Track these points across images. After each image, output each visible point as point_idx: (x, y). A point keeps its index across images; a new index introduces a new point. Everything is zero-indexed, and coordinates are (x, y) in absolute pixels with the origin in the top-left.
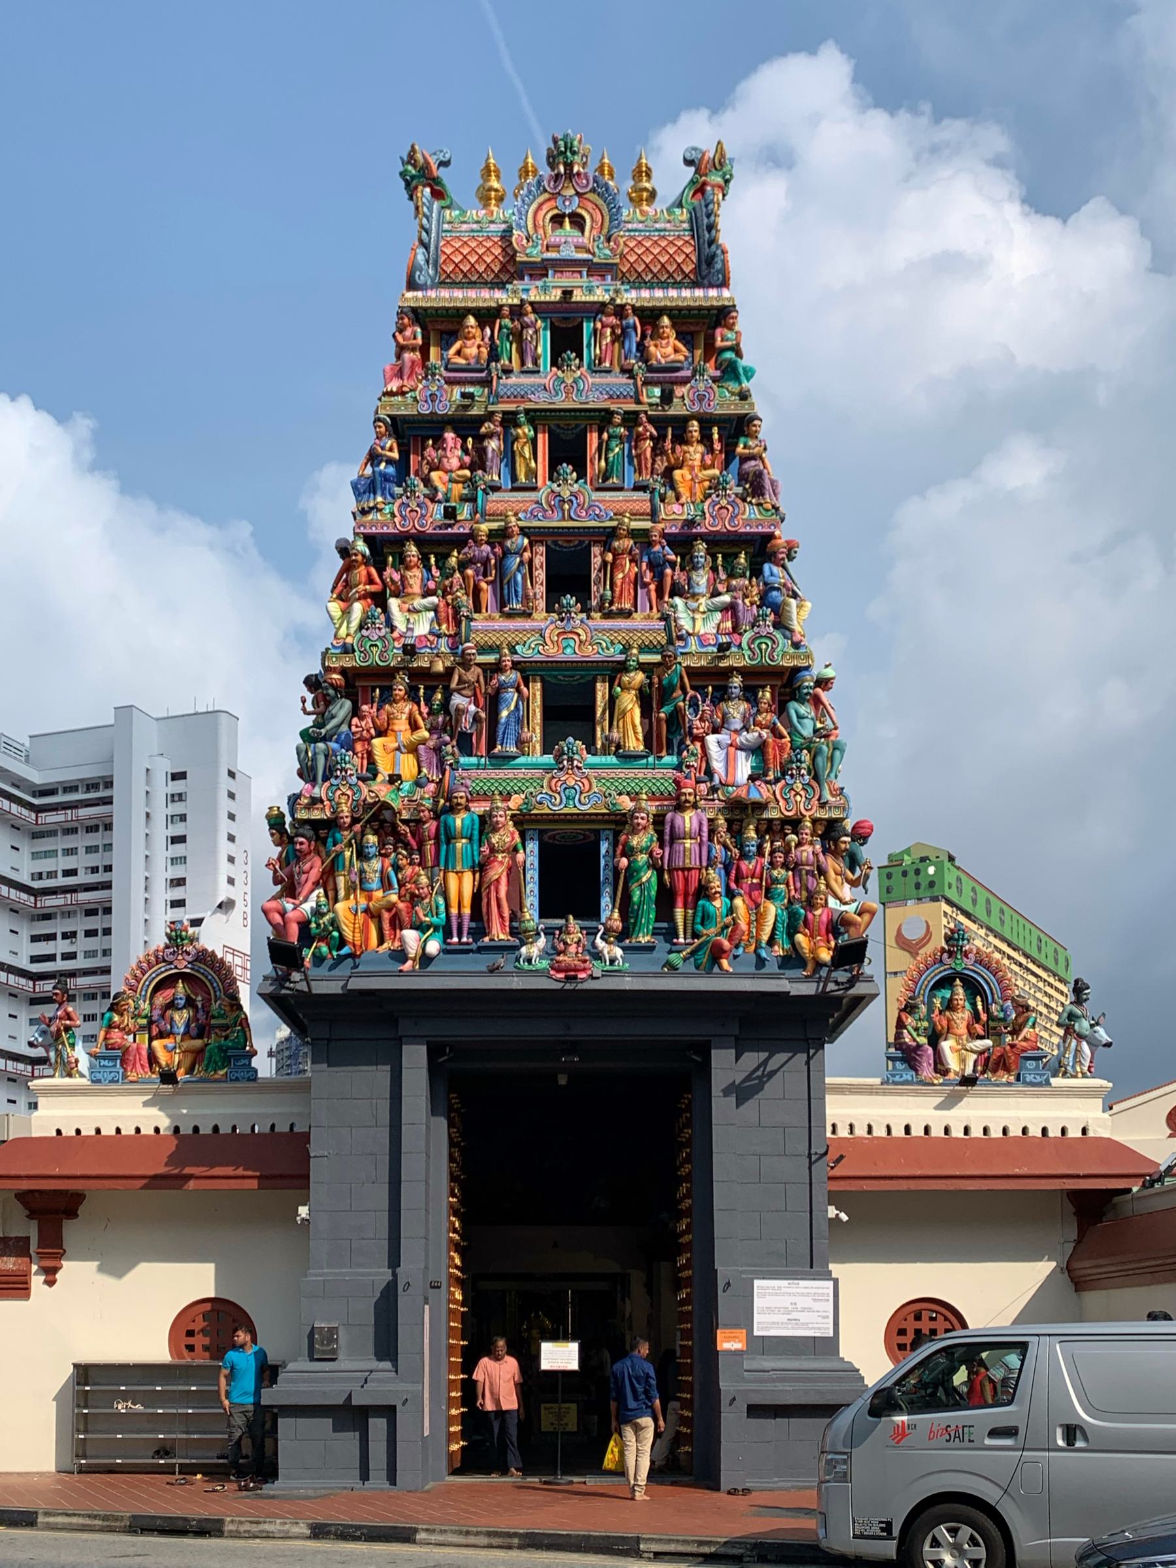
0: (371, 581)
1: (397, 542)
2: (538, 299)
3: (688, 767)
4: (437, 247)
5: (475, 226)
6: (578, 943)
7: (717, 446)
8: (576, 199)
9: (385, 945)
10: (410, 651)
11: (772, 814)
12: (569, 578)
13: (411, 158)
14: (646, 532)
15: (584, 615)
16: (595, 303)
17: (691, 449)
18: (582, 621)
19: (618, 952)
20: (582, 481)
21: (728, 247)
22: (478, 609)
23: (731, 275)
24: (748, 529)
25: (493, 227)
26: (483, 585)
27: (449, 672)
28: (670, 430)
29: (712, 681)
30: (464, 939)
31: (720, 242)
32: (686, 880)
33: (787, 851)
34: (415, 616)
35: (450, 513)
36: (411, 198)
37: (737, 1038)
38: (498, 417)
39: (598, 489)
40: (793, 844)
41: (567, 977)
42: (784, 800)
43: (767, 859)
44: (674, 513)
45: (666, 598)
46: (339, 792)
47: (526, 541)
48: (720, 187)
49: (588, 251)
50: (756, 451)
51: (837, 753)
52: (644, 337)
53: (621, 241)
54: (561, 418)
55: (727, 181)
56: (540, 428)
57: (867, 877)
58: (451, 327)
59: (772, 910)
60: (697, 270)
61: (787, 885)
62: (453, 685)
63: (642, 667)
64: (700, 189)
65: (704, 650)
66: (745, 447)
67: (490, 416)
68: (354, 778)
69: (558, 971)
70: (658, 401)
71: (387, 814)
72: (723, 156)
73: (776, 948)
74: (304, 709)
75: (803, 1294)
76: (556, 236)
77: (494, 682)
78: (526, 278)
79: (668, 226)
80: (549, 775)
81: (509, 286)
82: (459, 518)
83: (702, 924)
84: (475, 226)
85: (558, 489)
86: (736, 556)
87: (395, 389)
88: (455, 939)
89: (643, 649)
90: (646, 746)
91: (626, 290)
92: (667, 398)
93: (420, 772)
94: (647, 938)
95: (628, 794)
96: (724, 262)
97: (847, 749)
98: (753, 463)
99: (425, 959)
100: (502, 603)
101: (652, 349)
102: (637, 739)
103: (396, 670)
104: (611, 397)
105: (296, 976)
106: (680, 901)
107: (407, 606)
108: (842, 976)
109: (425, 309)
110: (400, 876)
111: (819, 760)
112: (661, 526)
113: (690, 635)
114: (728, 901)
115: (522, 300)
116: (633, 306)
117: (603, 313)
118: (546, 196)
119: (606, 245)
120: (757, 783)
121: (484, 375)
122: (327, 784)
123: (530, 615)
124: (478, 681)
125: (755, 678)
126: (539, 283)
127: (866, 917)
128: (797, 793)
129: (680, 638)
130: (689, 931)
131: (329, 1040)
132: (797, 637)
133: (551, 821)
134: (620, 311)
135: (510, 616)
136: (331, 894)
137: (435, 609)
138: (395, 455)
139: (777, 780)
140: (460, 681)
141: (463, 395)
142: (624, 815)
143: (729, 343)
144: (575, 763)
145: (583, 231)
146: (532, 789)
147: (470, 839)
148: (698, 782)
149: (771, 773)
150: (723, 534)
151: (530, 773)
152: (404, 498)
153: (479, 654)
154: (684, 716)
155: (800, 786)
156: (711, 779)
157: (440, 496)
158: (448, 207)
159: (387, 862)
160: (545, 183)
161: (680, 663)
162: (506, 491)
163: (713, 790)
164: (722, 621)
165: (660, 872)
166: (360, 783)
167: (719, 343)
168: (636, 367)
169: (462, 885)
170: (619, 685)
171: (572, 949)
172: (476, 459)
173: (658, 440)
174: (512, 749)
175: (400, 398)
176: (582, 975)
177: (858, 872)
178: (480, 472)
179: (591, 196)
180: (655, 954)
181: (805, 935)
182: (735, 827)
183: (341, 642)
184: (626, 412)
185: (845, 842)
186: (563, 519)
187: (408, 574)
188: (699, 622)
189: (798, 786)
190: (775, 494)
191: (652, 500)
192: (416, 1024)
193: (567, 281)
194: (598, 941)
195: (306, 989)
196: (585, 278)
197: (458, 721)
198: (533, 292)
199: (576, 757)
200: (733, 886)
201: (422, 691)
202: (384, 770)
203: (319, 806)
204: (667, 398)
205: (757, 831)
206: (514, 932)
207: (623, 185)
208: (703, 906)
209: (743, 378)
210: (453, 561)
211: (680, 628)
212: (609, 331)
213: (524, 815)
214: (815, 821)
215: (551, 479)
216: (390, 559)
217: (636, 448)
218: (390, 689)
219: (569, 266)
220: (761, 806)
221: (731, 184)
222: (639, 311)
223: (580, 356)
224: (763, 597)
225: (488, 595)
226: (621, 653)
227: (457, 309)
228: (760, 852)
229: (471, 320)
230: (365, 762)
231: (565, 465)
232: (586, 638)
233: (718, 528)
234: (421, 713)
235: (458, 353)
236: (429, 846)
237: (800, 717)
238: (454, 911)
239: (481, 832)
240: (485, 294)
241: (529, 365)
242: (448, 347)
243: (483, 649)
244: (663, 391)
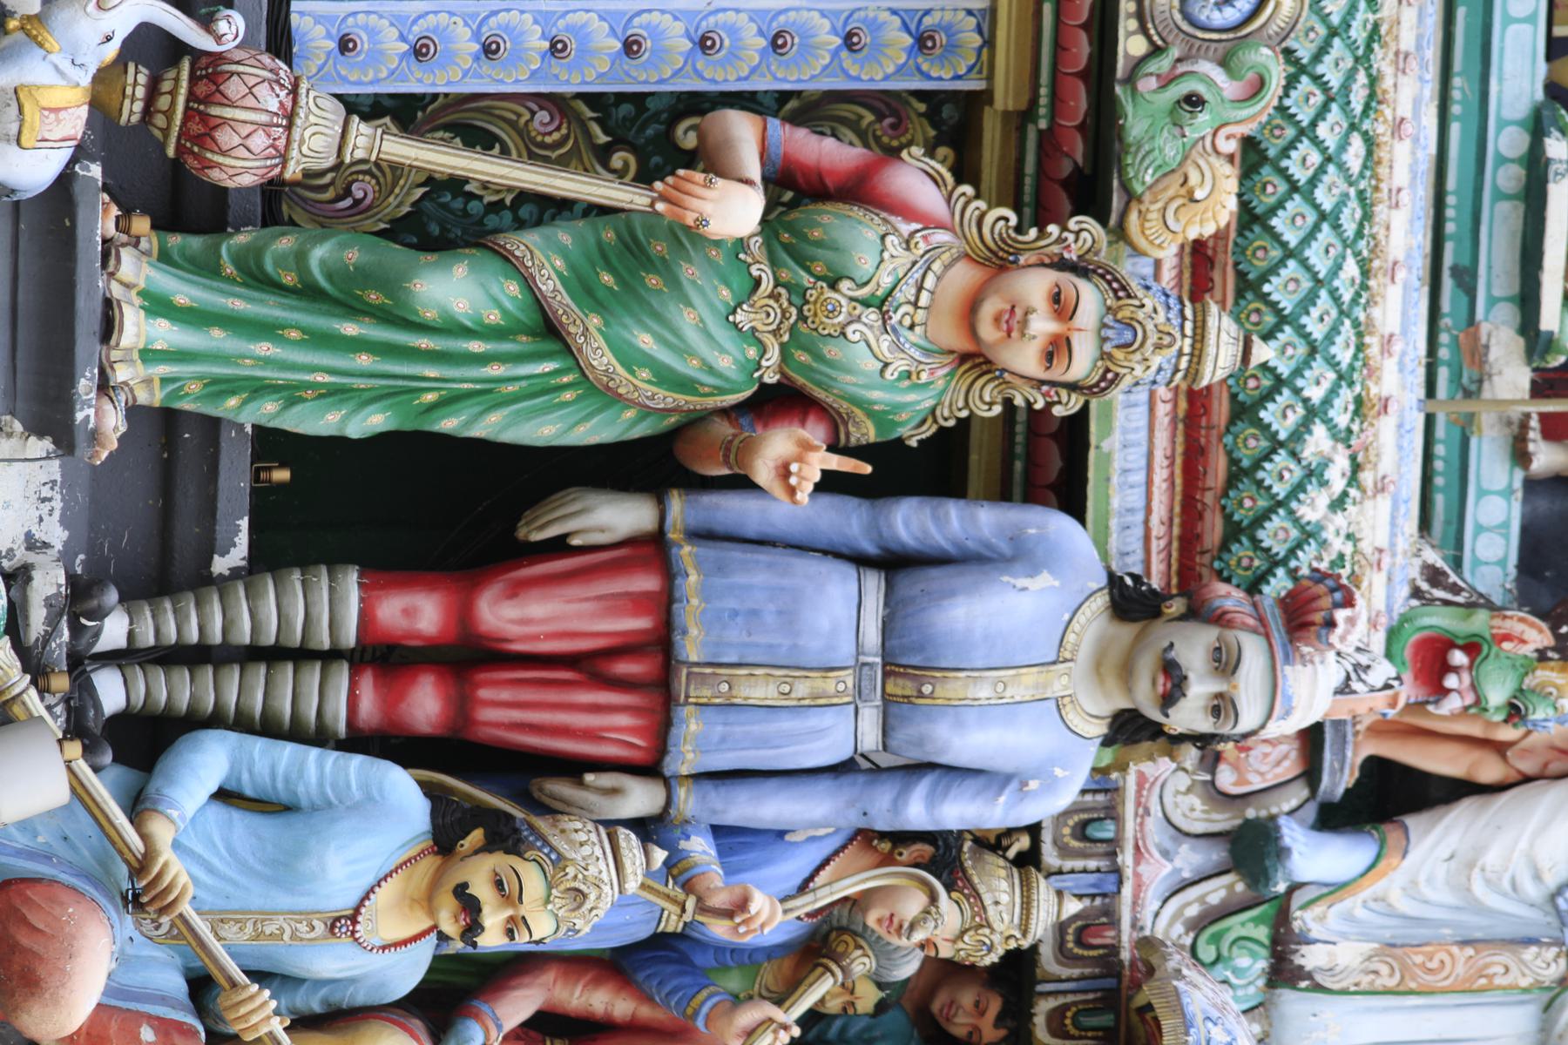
32: (588, 665)
130: (177, 690)
156: (1332, 818)
165: (649, 464)
208: (370, 803)
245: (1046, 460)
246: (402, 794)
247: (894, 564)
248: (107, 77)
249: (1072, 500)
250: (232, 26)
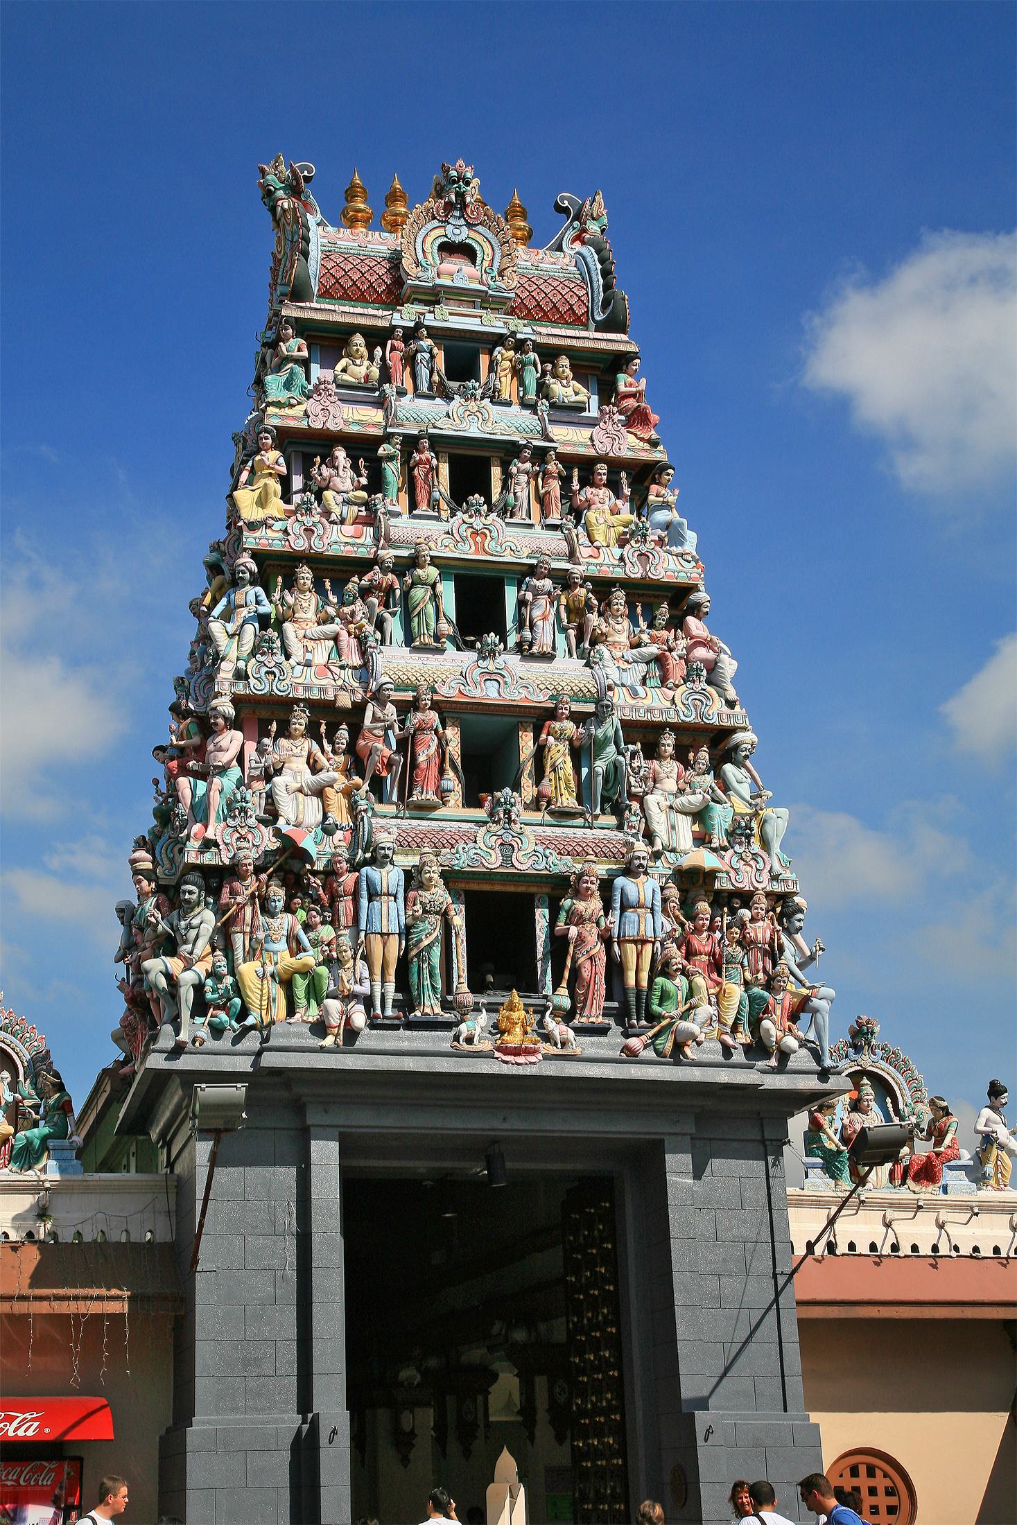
7: (627, 491)
27: (359, 708)
33: (743, 926)
52: (544, 373)
67: (387, 438)
83: (660, 1005)
89: (576, 699)
100: (409, 639)
112: (581, 568)
117: (502, 345)
118: (435, 223)
134: (520, 346)
145: (474, 263)
163: (657, 856)
173: (566, 481)
186: (477, 552)
203: (214, 849)
206: (446, 1006)
210: (352, 587)
219: (462, 295)
220: (712, 875)
222: (537, 347)
225: (394, 626)
232: (513, 680)
233: (639, 575)
234: (323, 751)
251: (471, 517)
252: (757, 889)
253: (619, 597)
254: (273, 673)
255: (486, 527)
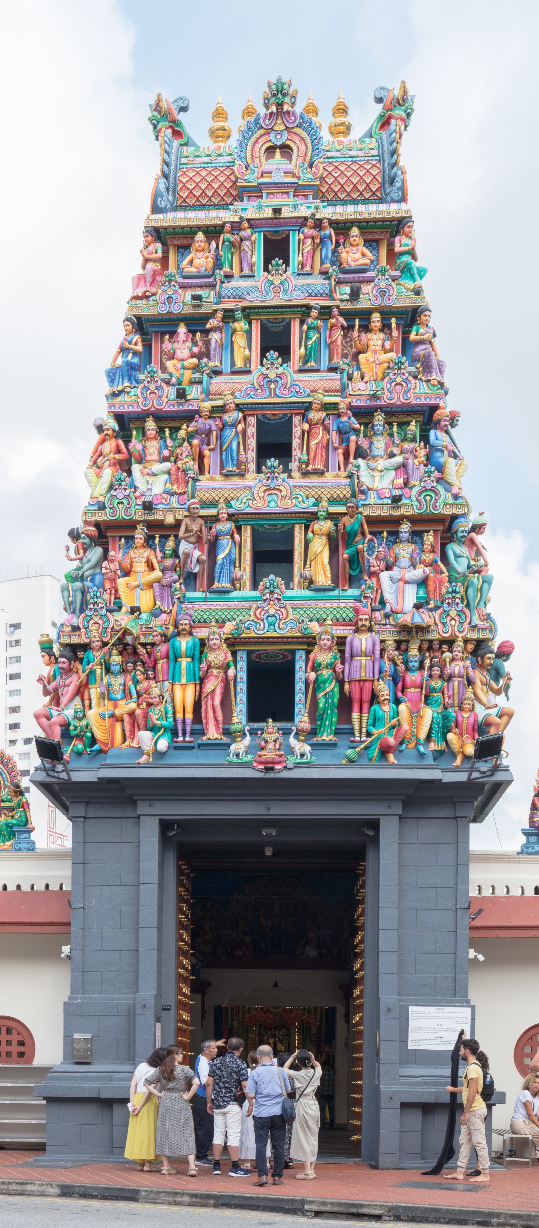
0: (119, 451)
1: (140, 418)
2: (254, 216)
3: (366, 597)
4: (175, 178)
5: (207, 159)
6: (275, 741)
8: (286, 132)
9: (127, 743)
10: (148, 507)
11: (433, 636)
12: (274, 446)
13: (158, 108)
14: (335, 405)
15: (286, 475)
16: (299, 218)
17: (374, 337)
18: (284, 480)
19: (307, 749)
20: (285, 365)
21: (407, 169)
22: (201, 471)
23: (409, 192)
24: (418, 402)
25: (220, 159)
26: (207, 452)
27: (178, 524)
28: (357, 320)
29: (385, 527)
30: (188, 739)
31: (401, 164)
33: (442, 665)
34: (153, 478)
35: (181, 395)
36: (157, 139)
37: (401, 817)
38: (219, 315)
39: (300, 371)
40: (448, 660)
41: (266, 769)
42: (441, 624)
43: (426, 673)
44: (361, 390)
45: (351, 460)
46: (92, 622)
47: (241, 415)
48: (402, 119)
49: (293, 175)
50: (425, 337)
51: (486, 585)
52: (338, 244)
53: (321, 166)
54: (270, 313)
55: (408, 115)
56: (254, 322)
57: (507, 687)
58: (185, 242)
59: (429, 714)
60: (382, 188)
61: (443, 693)
62: (181, 533)
63: (331, 516)
64: (385, 122)
65: (380, 502)
66: (417, 334)
68: (104, 611)
69: (261, 763)
70: (348, 297)
71: (129, 639)
72: (405, 93)
73: (432, 744)
74: (68, 556)
75: (447, 1018)
76: (268, 165)
77: (213, 530)
78: (245, 199)
79: (360, 153)
80: (255, 606)
81: (231, 207)
82: (188, 397)
84: (207, 159)
85: (266, 372)
86: (408, 423)
87: (140, 294)
88: (181, 739)
90: (333, 582)
91: (324, 207)
92: (355, 295)
93: (155, 604)
94: (329, 738)
95: (318, 620)
96: (403, 182)
97: (494, 582)
98: (424, 347)
99: (158, 755)
101: (344, 255)
102: (326, 576)
103: (139, 522)
104: (310, 295)
105: (60, 768)
106: (356, 707)
107: (146, 471)
108: (484, 766)
109: (166, 228)
110: (138, 688)
111: (471, 591)
112: (349, 400)
113: (369, 489)
114: (395, 706)
115: (241, 218)
116: (329, 219)
118: (262, 131)
119: (309, 170)
120: (421, 610)
121: (211, 280)
122: (83, 615)
123: (243, 475)
124: (201, 531)
125: (421, 523)
126: (255, 204)
127: (505, 719)
128: (453, 619)
129: (362, 492)
131: (85, 818)
132: (455, 490)
133: (257, 643)
135: (227, 476)
136: (87, 703)
137: (169, 473)
138: (139, 348)
139: (437, 608)
140: (187, 530)
141: (195, 297)
142: (314, 638)
143: (406, 248)
144: (276, 595)
146: (241, 617)
147: (193, 658)
148: (373, 610)
149: (432, 602)
150: (399, 406)
151: (240, 605)
152: (146, 383)
153: (202, 508)
154: (363, 556)
155: (455, 613)
157: (174, 380)
158: (186, 145)
159: (129, 677)
160: (261, 121)
161: (361, 513)
162: (227, 374)
163: (387, 616)
164: (396, 478)
165: (341, 683)
166: (108, 614)
167: (397, 249)
168: (331, 270)
169: (185, 695)
170: (313, 532)
171: (271, 746)
172: (203, 349)
174: (227, 585)
175: (144, 301)
176: (278, 767)
177: (502, 682)
178: (205, 360)
179: (298, 131)
180: (337, 751)
181: (455, 734)
182: (403, 647)
183: (96, 500)
184: (322, 307)
185: (490, 658)
186: (270, 396)
187: (148, 444)
188: (379, 478)
189: (453, 613)
190: (441, 372)
191: (341, 379)
192: (150, 806)
193: (277, 201)
194: (292, 740)
195: (66, 778)
196: (292, 198)
197: (185, 563)
198: (250, 210)
199: (276, 590)
200: (400, 694)
201: (157, 539)
202: (127, 602)
204: (355, 295)
205: (420, 649)
206: (227, 732)
207: (324, 121)
209: (417, 277)
210: (182, 433)
211: (360, 484)
212: (309, 241)
213: (235, 639)
214: (466, 641)
215: (262, 364)
216: (134, 433)
217: (330, 336)
218: (132, 538)
220: (422, 629)
221: (412, 117)
223: (287, 262)
224: (428, 458)
226: (314, 505)
227: (191, 227)
228: (421, 666)
229: (200, 236)
230: (113, 597)
231: (272, 352)
233: (394, 401)
234: (156, 557)
235: (191, 262)
236: (161, 664)
237: (457, 556)
238: (179, 716)
239: (201, 653)
240: (213, 214)
241: (247, 271)
242: (183, 257)
243: (205, 504)
244: (352, 289)
245: (341, 641)
246: (373, 708)
247: (352, 656)
248: (299, 740)
249: (345, 638)
250: (293, 728)
251: (268, 369)
252: (458, 637)
253: (379, 419)
254: (122, 503)
255: (278, 376)
